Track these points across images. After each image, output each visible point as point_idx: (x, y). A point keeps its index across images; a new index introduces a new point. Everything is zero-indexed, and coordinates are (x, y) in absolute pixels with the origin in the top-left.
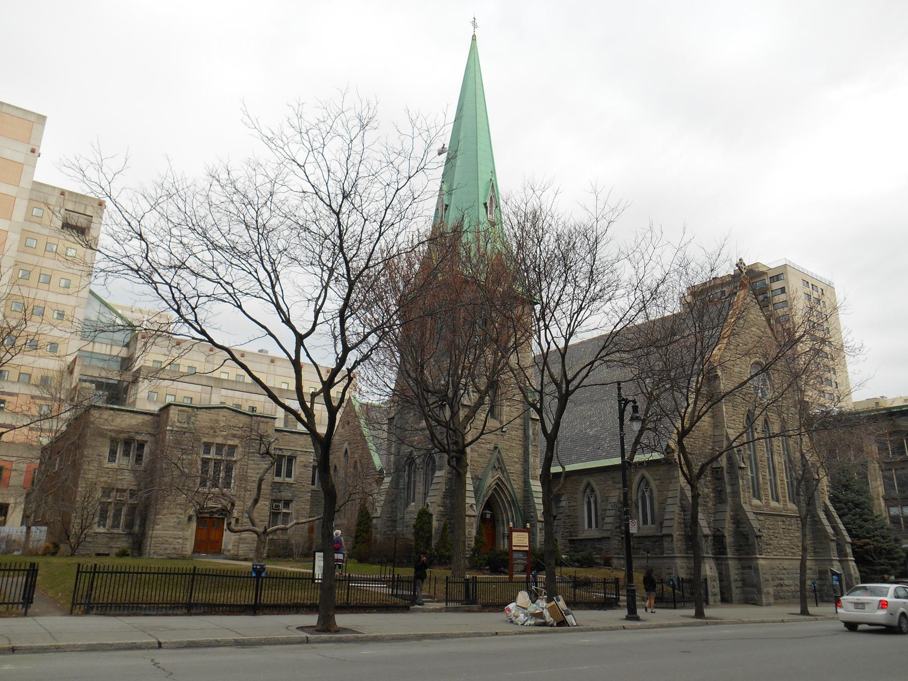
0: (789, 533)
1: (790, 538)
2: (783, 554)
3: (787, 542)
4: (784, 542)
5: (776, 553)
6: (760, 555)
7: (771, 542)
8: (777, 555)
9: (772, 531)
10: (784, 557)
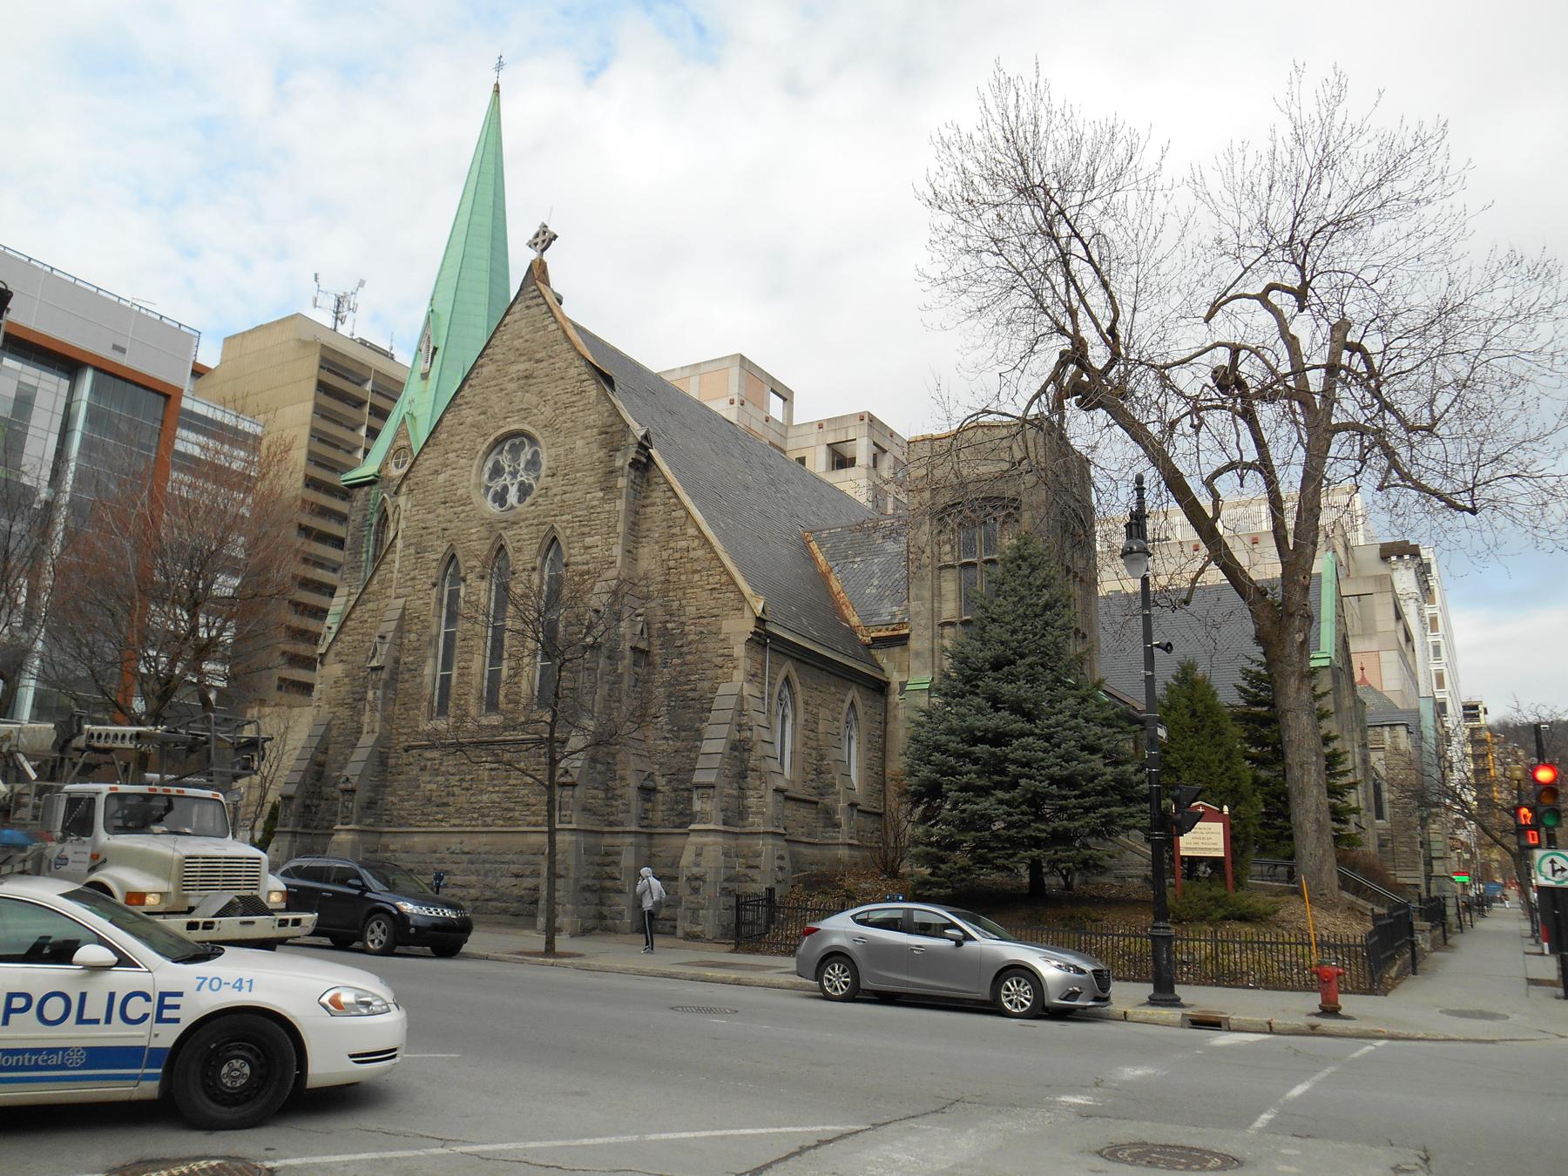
0: (508, 777)
1: (503, 788)
3: (495, 797)
4: (485, 797)
5: (457, 822)
6: (342, 824)
8: (460, 825)
9: (457, 778)
10: (477, 829)
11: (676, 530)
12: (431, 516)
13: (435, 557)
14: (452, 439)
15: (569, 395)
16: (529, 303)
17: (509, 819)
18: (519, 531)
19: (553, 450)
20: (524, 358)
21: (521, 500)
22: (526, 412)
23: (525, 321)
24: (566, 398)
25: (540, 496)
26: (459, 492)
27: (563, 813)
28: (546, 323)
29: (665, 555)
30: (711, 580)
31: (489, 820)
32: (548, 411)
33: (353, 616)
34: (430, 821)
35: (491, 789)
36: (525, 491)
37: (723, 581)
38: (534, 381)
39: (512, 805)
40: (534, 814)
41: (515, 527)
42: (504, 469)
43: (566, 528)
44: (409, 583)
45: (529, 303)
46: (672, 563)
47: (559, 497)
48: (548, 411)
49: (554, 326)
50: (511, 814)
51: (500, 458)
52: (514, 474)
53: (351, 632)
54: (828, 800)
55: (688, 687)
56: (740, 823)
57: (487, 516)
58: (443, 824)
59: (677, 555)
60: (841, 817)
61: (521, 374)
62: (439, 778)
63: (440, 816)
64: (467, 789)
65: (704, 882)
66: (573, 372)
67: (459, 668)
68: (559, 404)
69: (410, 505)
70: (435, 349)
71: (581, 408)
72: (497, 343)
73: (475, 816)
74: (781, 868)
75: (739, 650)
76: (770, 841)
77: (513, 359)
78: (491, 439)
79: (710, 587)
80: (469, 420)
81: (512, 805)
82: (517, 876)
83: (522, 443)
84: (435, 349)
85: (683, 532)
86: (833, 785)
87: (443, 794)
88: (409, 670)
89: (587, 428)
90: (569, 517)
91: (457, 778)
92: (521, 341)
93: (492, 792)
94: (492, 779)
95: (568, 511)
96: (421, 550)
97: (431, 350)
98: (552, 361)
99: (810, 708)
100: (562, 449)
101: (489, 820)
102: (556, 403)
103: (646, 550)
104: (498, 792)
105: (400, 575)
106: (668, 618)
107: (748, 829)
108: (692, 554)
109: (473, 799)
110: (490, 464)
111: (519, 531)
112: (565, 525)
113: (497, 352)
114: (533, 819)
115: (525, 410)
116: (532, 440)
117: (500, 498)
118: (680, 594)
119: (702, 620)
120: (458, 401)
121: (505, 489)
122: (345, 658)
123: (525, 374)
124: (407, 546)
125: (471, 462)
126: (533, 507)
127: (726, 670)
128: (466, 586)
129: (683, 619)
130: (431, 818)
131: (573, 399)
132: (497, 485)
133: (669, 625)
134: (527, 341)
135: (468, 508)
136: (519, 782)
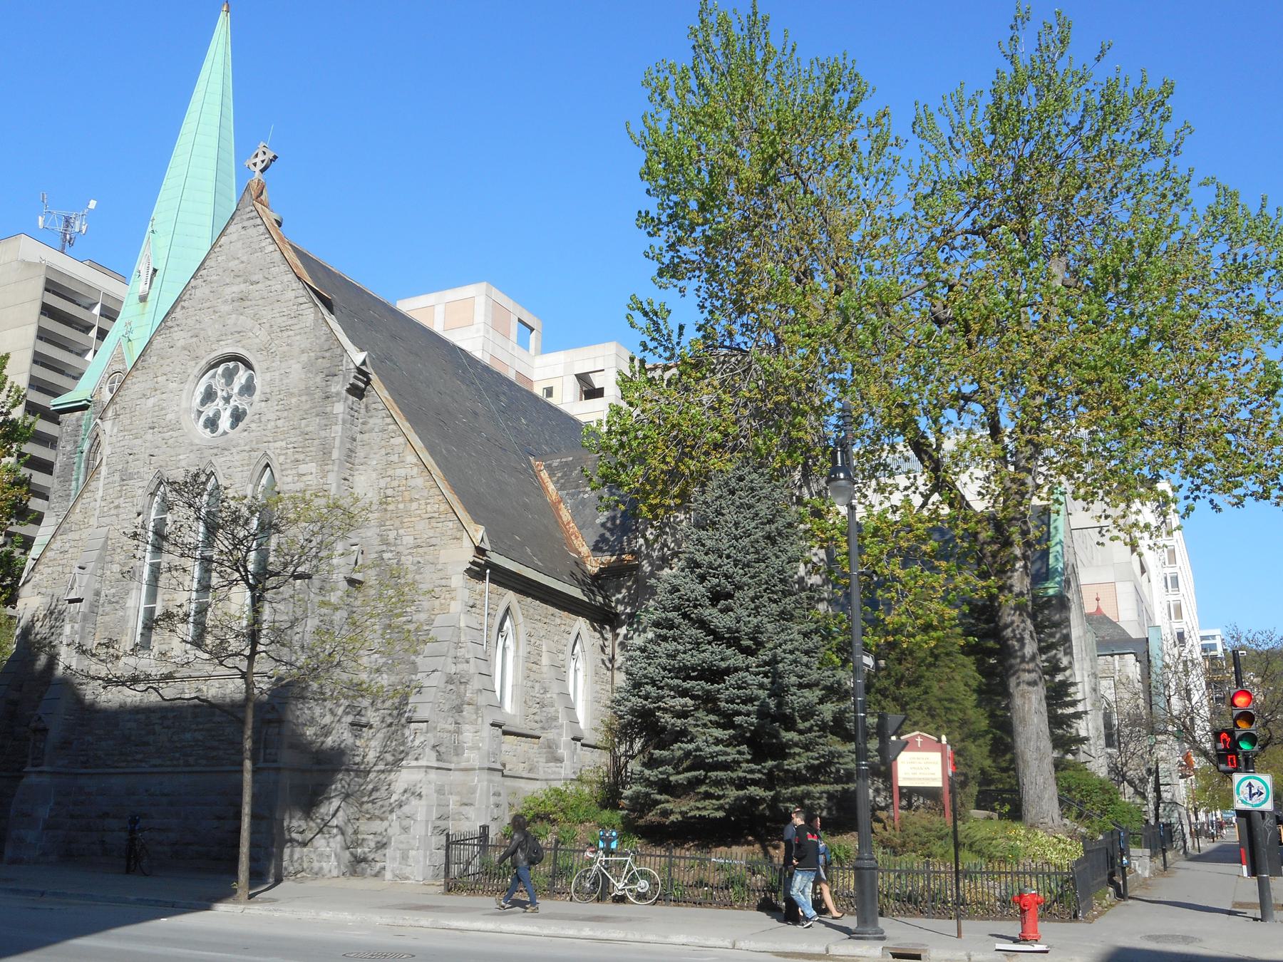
2: (181, 762)
3: (199, 736)
4: (188, 736)
5: (158, 762)
6: (33, 766)
10: (179, 769)
11: (395, 458)
12: (139, 442)
13: (141, 484)
14: (162, 362)
15: (285, 318)
16: (246, 224)
19: (268, 374)
20: (240, 279)
21: (234, 426)
23: (241, 242)
24: (281, 321)
25: (253, 421)
26: (169, 417)
27: (268, 751)
28: (263, 244)
29: (383, 483)
30: (429, 509)
31: (191, 760)
32: (263, 335)
33: (53, 546)
35: (194, 727)
36: (238, 417)
37: (441, 509)
38: (249, 303)
41: (226, 453)
42: (216, 393)
43: (279, 455)
44: (113, 512)
45: (246, 224)
46: (389, 492)
47: (273, 423)
48: (263, 335)
49: (272, 248)
50: (215, 753)
51: (212, 381)
52: (227, 400)
53: (50, 564)
54: (550, 735)
55: (404, 619)
56: (455, 759)
57: (197, 441)
58: (143, 764)
59: (395, 483)
60: (563, 752)
63: (139, 757)
64: (168, 727)
65: (415, 821)
66: (291, 295)
67: (163, 600)
68: (275, 327)
69: (115, 430)
70: (155, 271)
71: (297, 332)
73: (177, 755)
74: (497, 806)
75: (458, 580)
76: (485, 775)
78: (203, 363)
79: (428, 516)
80: (181, 343)
82: (219, 818)
83: (236, 369)
84: (155, 271)
85: (401, 459)
86: (556, 719)
88: (110, 602)
89: (303, 352)
90: (283, 444)
92: (237, 262)
93: (195, 730)
95: (282, 437)
96: (126, 477)
97: (151, 271)
98: (268, 283)
99: (533, 640)
100: (277, 373)
101: (191, 760)
103: (362, 478)
104: (202, 730)
105: (103, 504)
106: (384, 548)
107: (463, 765)
108: (411, 483)
109: (175, 738)
110: (201, 388)
112: (278, 451)
113: (210, 273)
115: (239, 332)
116: (249, 366)
117: (212, 424)
118: (397, 523)
119: (420, 550)
120: (169, 324)
121: (217, 415)
122: (43, 590)
123: (240, 296)
124: (111, 474)
126: (246, 433)
127: (443, 601)
129: (400, 549)
130: (130, 758)
131: (290, 322)
132: (209, 410)
133: (386, 556)
134: (242, 262)
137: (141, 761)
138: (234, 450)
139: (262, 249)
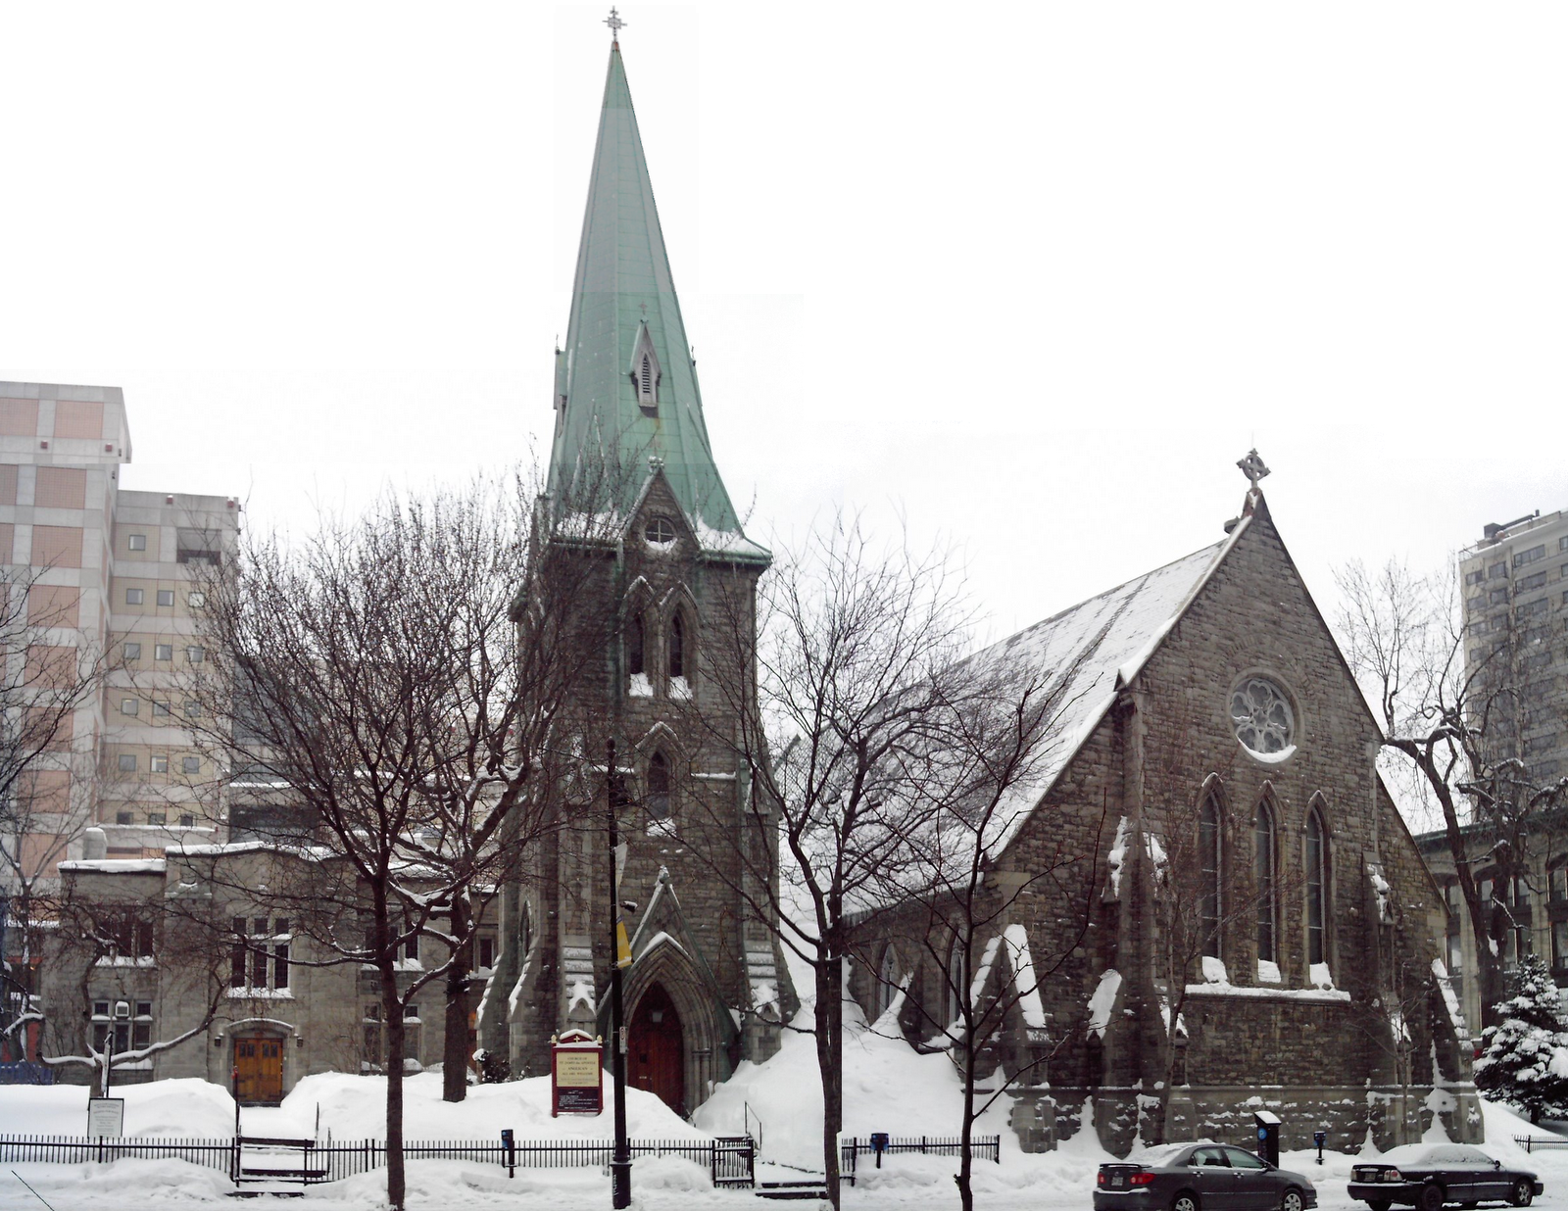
1: (1297, 1047)
4: (1280, 1055)
7: (1243, 1057)
15: (1318, 664)
17: (1305, 1078)
18: (1284, 787)
22: (1280, 665)
34: (1222, 1079)
39: (1307, 1064)
40: (1327, 1073)
49: (1293, 581)
58: (1237, 1082)
61: (1269, 617)
62: (1228, 1033)
72: (1235, 564)
73: (1271, 1074)
77: (1257, 594)
81: (1307, 1064)
87: (1234, 1050)
89: (1339, 707)
91: (1247, 1034)
92: (1260, 577)
94: (1283, 1037)
102: (1306, 666)
109: (1267, 1057)
111: (1284, 787)
114: (1328, 1078)
125: (1224, 690)
126: (1297, 768)
128: (1234, 828)
135: (1227, 742)
136: (1311, 1042)
137: (1236, 1079)
138: (1287, 781)
139: (1285, 577)
